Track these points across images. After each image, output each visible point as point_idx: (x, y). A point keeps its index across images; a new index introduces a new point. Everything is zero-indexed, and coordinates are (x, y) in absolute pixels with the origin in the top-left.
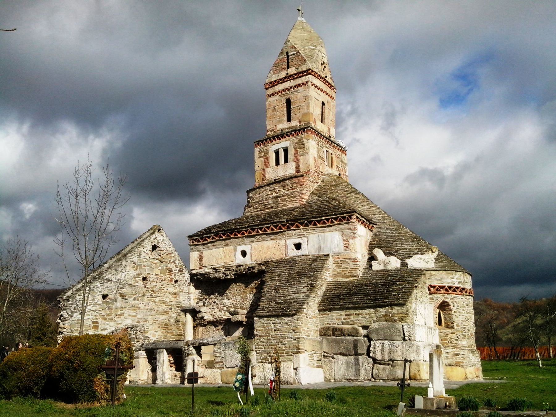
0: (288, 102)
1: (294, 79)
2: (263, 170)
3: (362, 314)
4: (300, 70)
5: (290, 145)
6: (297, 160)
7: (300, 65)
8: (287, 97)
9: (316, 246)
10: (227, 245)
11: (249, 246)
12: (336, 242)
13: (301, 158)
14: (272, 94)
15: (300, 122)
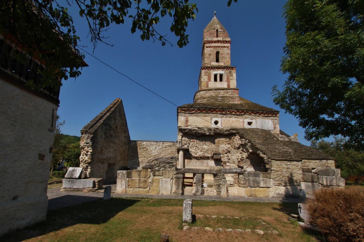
0: (218, 53)
1: (223, 43)
2: (207, 82)
3: (312, 162)
4: (224, 40)
5: (224, 73)
6: (228, 81)
7: (225, 37)
8: (218, 50)
9: (261, 125)
10: (206, 116)
11: (221, 119)
12: (270, 124)
13: (231, 81)
14: (208, 47)
15: (224, 64)
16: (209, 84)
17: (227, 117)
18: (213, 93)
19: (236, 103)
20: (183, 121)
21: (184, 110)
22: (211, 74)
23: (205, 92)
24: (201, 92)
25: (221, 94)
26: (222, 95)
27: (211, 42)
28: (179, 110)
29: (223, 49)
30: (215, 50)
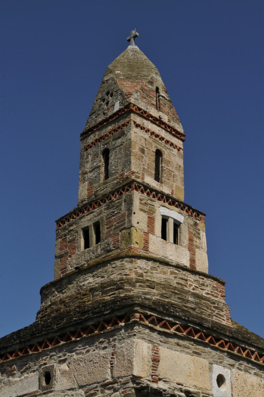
2: (146, 234)
8: (159, 147)
13: (197, 250)
16: (150, 242)
17: (241, 370)
18: (172, 277)
19: (224, 323)
20: (146, 360)
21: (151, 316)
22: (154, 212)
23: (150, 263)
24: (138, 261)
25: (191, 285)
26: (194, 289)
27: (145, 115)
28: (138, 315)
29: (170, 150)
30: (154, 145)
